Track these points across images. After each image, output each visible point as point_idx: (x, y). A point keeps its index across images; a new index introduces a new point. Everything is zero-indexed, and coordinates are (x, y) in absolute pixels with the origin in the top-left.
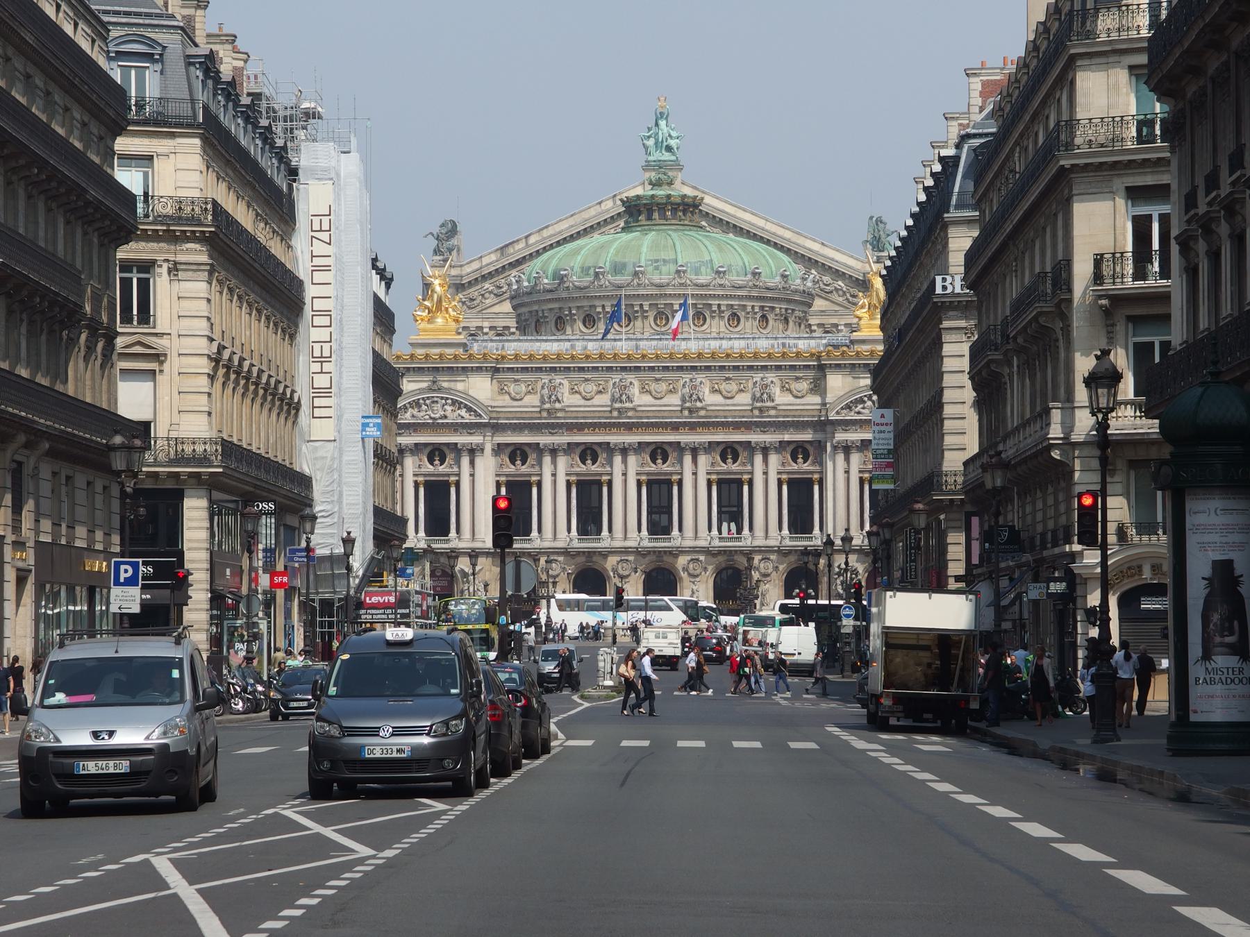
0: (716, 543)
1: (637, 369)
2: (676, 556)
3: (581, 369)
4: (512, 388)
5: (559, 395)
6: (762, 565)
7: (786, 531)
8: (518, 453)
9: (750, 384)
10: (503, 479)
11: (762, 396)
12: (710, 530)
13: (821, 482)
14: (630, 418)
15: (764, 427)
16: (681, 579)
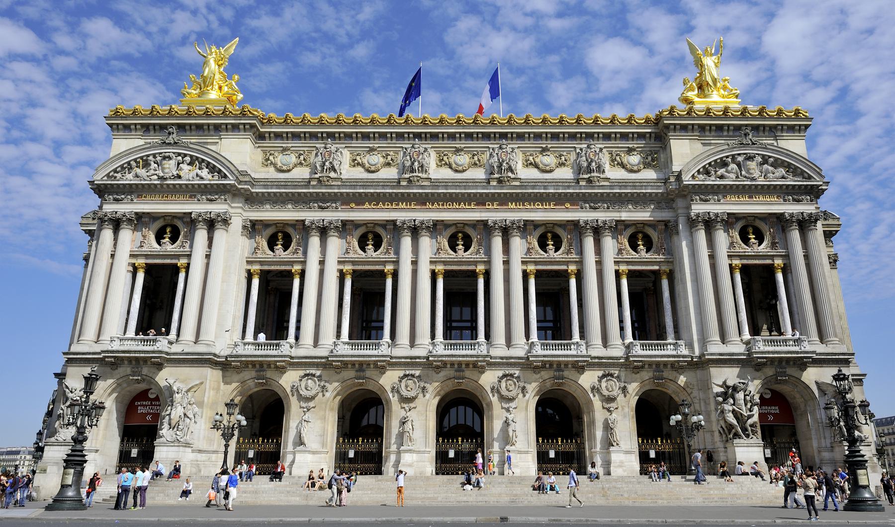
0: (538, 350)
1: (434, 136)
2: (481, 370)
3: (366, 136)
4: (280, 159)
5: (335, 163)
6: (604, 384)
7: (629, 339)
8: (280, 235)
9: (573, 157)
10: (256, 268)
11: (586, 170)
12: (527, 336)
13: (671, 276)
14: (422, 187)
15: (593, 201)
16: (490, 404)
